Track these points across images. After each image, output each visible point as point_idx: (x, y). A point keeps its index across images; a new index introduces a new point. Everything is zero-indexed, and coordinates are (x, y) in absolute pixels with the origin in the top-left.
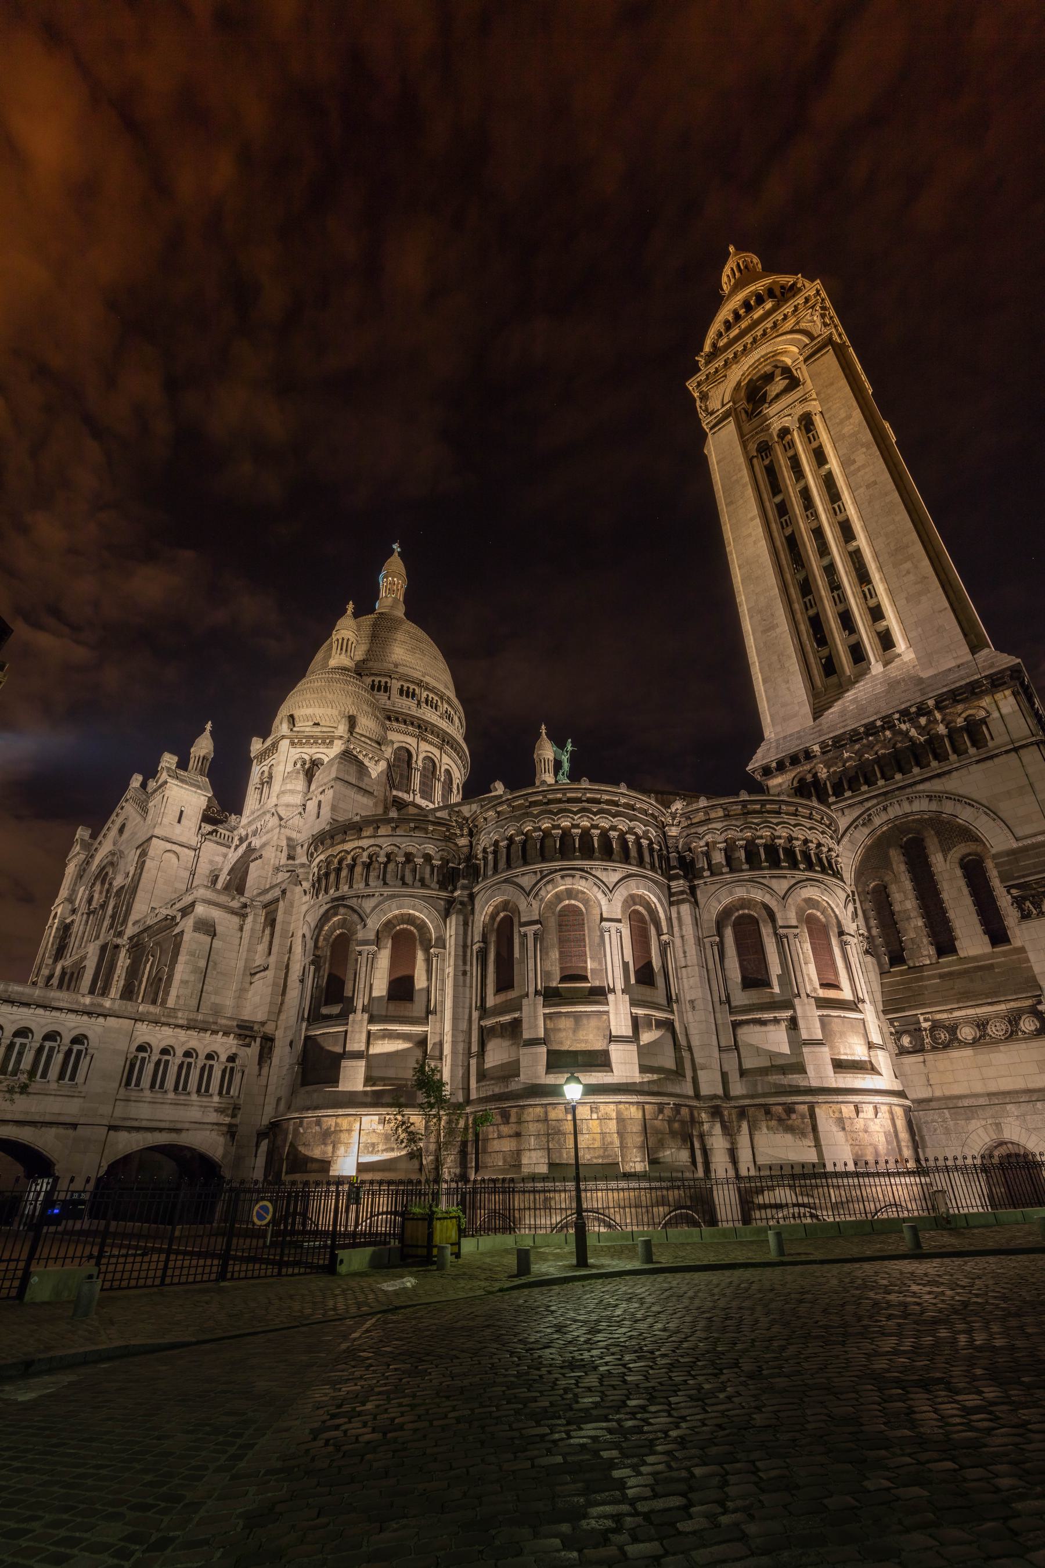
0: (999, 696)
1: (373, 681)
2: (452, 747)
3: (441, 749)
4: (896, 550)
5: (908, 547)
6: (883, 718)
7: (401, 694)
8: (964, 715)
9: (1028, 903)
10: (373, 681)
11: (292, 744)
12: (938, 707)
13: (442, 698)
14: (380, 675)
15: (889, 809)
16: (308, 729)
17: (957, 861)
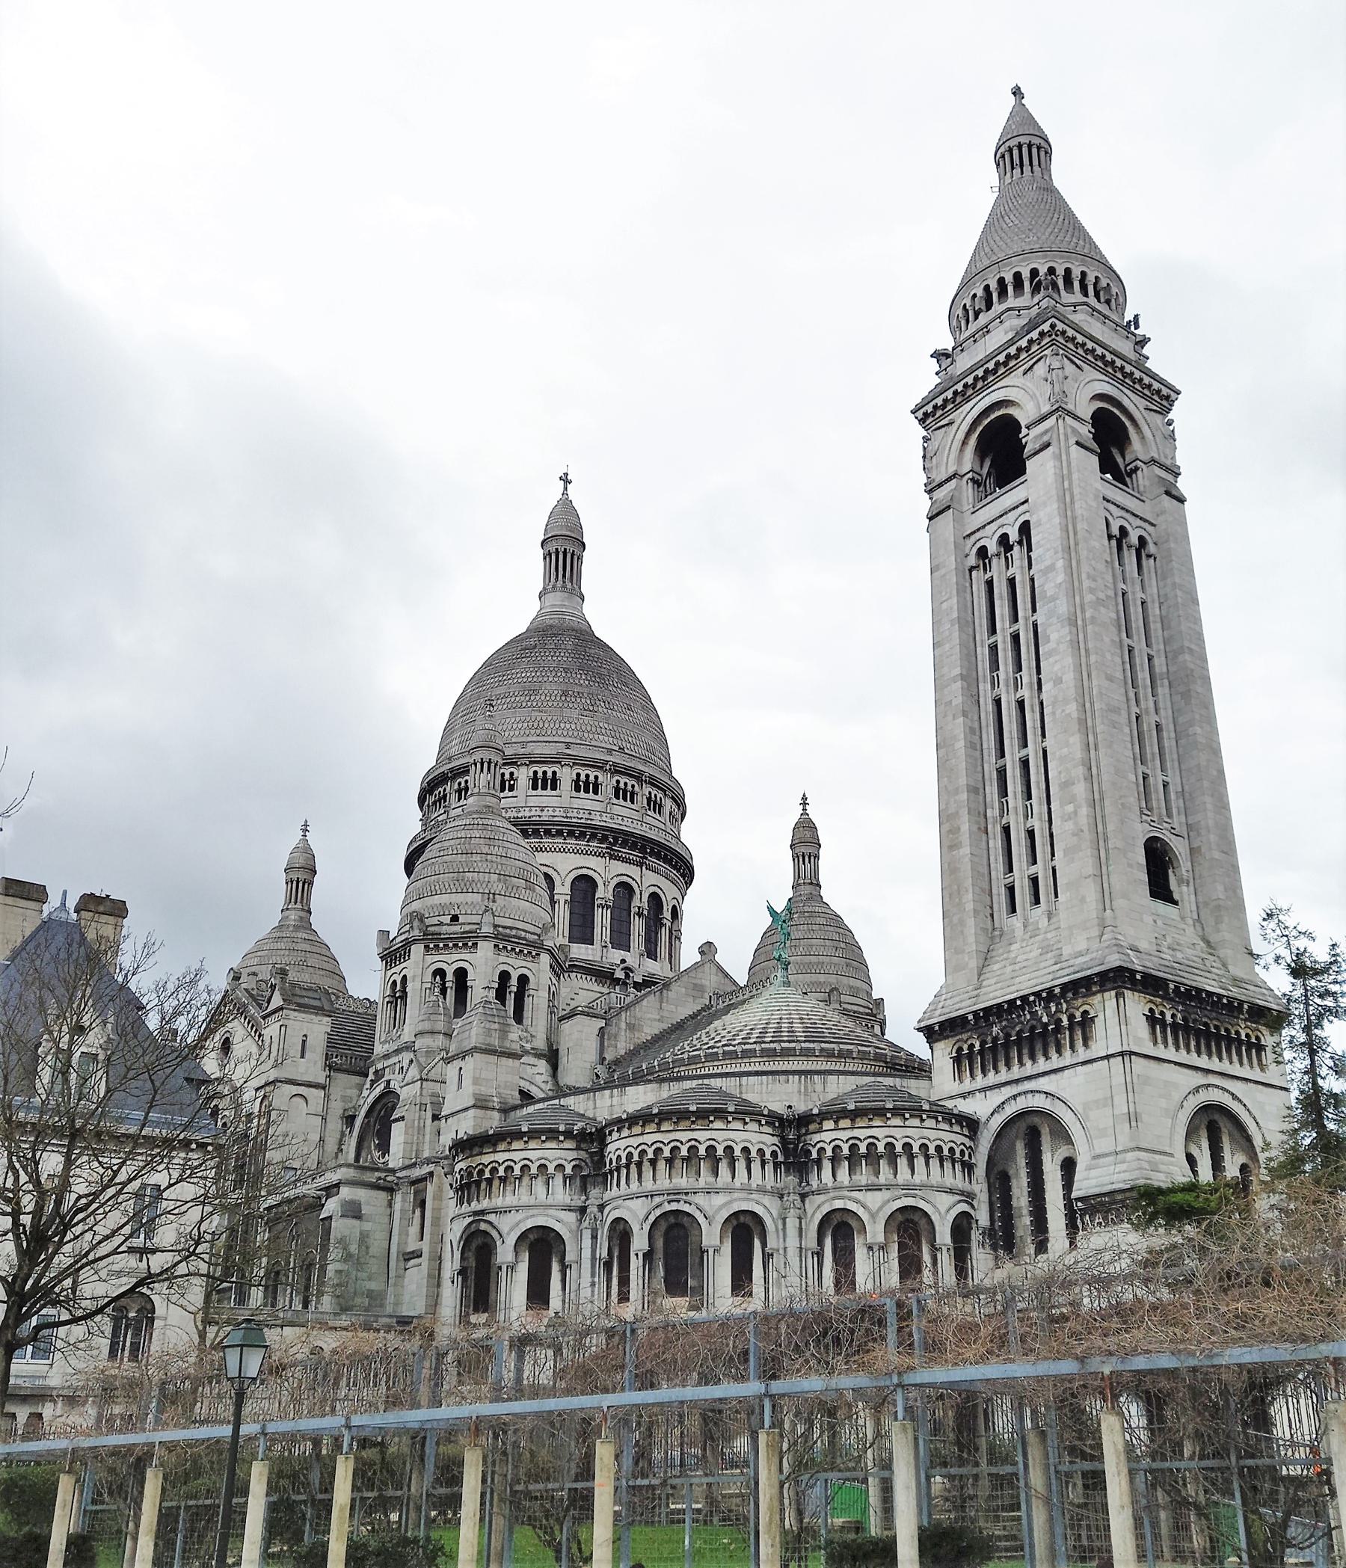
0: (1107, 994)
1: (535, 773)
7: (577, 789)
8: (1081, 1010)
9: (1087, 1217)
10: (535, 773)
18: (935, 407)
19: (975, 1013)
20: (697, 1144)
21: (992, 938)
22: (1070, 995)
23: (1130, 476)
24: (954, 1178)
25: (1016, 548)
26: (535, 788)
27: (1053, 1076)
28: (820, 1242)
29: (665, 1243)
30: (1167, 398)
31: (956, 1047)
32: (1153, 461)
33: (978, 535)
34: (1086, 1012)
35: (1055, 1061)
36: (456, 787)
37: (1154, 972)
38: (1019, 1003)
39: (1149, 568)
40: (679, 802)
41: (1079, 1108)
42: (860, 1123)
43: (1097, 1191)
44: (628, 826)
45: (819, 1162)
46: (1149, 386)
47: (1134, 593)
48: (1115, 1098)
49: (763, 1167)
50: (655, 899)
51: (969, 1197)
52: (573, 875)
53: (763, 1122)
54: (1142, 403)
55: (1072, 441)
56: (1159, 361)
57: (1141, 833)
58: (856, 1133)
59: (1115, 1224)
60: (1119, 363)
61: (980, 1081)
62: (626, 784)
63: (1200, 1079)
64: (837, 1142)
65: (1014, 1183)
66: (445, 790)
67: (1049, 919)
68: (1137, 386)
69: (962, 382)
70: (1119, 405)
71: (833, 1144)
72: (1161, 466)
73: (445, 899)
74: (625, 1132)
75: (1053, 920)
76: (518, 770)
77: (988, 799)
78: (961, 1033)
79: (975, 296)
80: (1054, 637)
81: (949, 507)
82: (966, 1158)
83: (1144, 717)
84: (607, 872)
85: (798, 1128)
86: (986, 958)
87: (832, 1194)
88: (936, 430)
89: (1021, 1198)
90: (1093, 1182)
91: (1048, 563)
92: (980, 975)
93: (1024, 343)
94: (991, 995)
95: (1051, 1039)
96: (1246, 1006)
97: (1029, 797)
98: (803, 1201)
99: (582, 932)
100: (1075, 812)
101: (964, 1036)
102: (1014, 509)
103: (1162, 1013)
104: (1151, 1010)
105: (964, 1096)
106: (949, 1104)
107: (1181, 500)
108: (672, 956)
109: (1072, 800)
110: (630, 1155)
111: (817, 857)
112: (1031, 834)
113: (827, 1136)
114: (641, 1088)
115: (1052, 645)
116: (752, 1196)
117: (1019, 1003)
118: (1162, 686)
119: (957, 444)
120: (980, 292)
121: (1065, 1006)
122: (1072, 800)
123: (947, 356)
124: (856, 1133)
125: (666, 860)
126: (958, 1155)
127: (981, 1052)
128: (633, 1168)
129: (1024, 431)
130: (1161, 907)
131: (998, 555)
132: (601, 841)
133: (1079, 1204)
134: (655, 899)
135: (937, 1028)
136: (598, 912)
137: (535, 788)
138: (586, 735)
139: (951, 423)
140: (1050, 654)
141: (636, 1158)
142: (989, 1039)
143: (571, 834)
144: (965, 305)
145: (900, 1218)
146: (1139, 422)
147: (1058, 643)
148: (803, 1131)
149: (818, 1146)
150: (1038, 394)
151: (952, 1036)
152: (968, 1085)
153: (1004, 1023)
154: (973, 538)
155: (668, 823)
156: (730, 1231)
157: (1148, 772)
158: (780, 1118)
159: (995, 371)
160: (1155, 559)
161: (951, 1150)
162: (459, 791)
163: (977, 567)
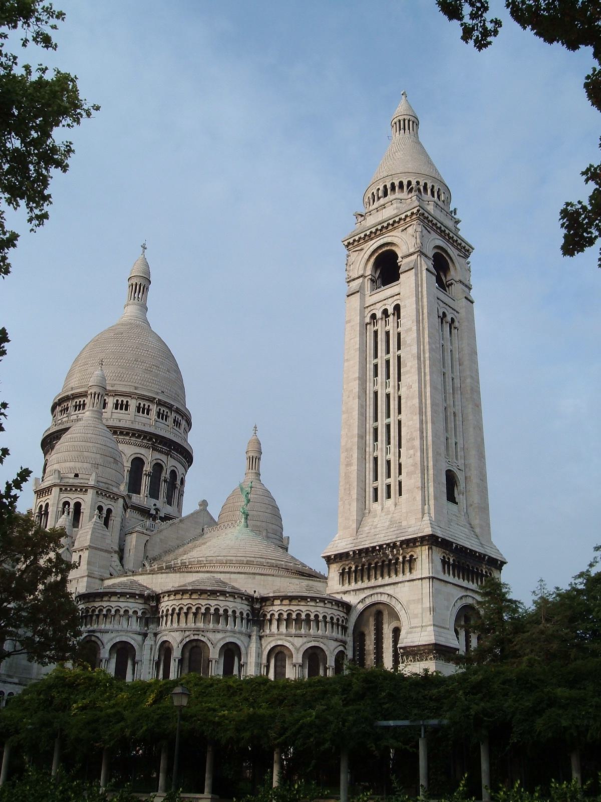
0: (423, 548)
1: (117, 401)
3: (167, 454)
4: (409, 439)
5: (414, 440)
7: (139, 412)
8: (410, 554)
9: (405, 657)
10: (117, 401)
11: (61, 489)
12: (401, 546)
16: (71, 481)
17: (392, 629)
18: (354, 241)
19: (354, 552)
20: (210, 607)
21: (364, 514)
22: (404, 546)
23: (448, 287)
24: (337, 634)
25: (391, 317)
26: (116, 408)
27: (392, 586)
28: (268, 661)
29: (190, 655)
30: (468, 251)
31: (342, 568)
32: (461, 282)
33: (372, 307)
34: (412, 556)
35: (394, 579)
36: (74, 404)
37: (447, 538)
38: (377, 548)
39: (455, 334)
40: (189, 424)
41: (405, 603)
42: (294, 603)
43: (412, 644)
44: (162, 433)
45: (270, 621)
46: (460, 244)
47: (447, 346)
48: (424, 599)
49: (242, 622)
50: (173, 473)
51: (344, 643)
52: (133, 457)
53: (244, 598)
54: (457, 252)
55: (424, 268)
56: (465, 232)
57: (444, 467)
58: (291, 608)
59: (419, 661)
60: (447, 231)
61: (353, 586)
62: (164, 411)
63: (463, 593)
65: (367, 638)
66: (68, 405)
67: (395, 506)
68: (455, 244)
69: (370, 230)
70: (446, 252)
71: (279, 612)
72: (463, 284)
73: (72, 464)
74: (172, 597)
75: (398, 507)
76: (108, 398)
77: (367, 442)
78: (345, 561)
79: (379, 189)
80: (409, 364)
81: (358, 292)
82: (344, 624)
83: (448, 409)
84: (150, 457)
85: (261, 603)
86: (360, 523)
87: (276, 637)
88: (353, 252)
89: (370, 645)
90: (409, 640)
91: (408, 327)
92: (357, 532)
93: (403, 216)
94: (363, 544)
95: (392, 567)
96: (487, 557)
97: (389, 443)
98: (260, 639)
99: (134, 487)
100: (414, 455)
101: (347, 562)
102: (391, 297)
103: (449, 559)
104: (444, 557)
105: (345, 593)
106: (338, 597)
107: (472, 302)
108: (179, 505)
109: (413, 447)
110: (174, 610)
111: (259, 459)
112: (388, 462)
113: (276, 608)
114: (178, 575)
115: (408, 368)
116: (236, 635)
117: (377, 548)
118: (457, 394)
119: (364, 261)
120: (382, 188)
121: (401, 551)
122: (413, 447)
123: (362, 216)
124: (291, 608)
125: (182, 455)
126: (340, 622)
127: (356, 571)
128: (175, 616)
129: (400, 259)
130: (450, 504)
131: (382, 319)
132: (149, 440)
133: (401, 650)
134: (173, 473)
135: (333, 557)
136: (144, 478)
137: (116, 408)
138: (145, 383)
139: (362, 250)
140: (407, 372)
141: (177, 611)
142: (360, 565)
143: (133, 435)
144: (373, 193)
145: (310, 651)
146: (455, 263)
147: (411, 367)
148: (264, 604)
149: (271, 612)
150: (409, 242)
151: (340, 562)
152: (347, 587)
153: (369, 558)
154: (369, 309)
155: (183, 434)
156: (224, 651)
157: (448, 436)
158: (252, 597)
159: (387, 228)
160: (458, 330)
161: (338, 620)
162: (76, 406)
163: (370, 323)
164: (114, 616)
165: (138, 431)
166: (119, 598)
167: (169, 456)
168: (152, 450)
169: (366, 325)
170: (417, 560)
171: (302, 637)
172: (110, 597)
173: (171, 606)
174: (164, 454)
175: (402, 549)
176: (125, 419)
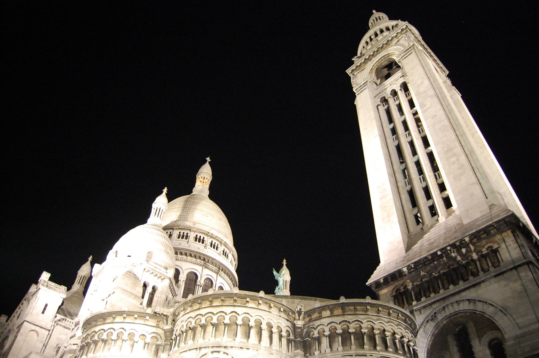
1: (180, 233)
2: (225, 273)
4: (448, 151)
5: (453, 149)
6: (441, 250)
7: (196, 241)
8: (486, 247)
10: (180, 233)
13: (221, 243)
14: (184, 229)
15: (446, 309)
27: (472, 290)
38: (439, 253)
45: (319, 340)
49: (280, 340)
53: (282, 310)
64: (332, 324)
109: (454, 155)
113: (325, 321)
122: (454, 155)
137: (179, 238)
143: (191, 255)
164: (115, 341)
165: (194, 252)
166: (124, 318)
167: (218, 275)
168: (205, 268)
169: (378, 105)
170: (499, 249)
171: (366, 355)
172: (114, 318)
173: (186, 320)
174: (214, 272)
175: (473, 244)
176: (183, 244)
